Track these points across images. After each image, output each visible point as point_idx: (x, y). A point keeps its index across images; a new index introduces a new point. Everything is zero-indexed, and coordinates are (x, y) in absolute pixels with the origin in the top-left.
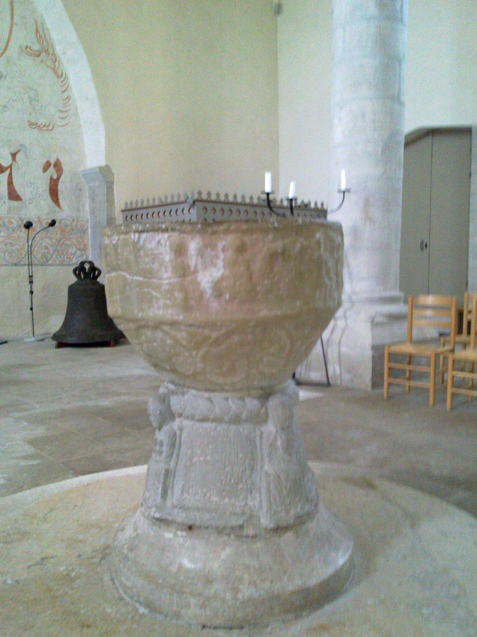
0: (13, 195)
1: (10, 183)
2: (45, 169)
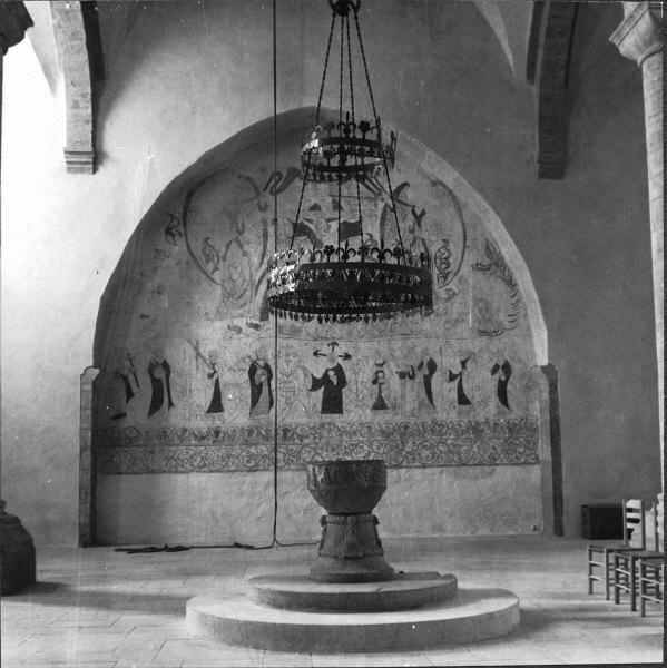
0: (463, 399)
1: (460, 388)
2: (494, 371)
